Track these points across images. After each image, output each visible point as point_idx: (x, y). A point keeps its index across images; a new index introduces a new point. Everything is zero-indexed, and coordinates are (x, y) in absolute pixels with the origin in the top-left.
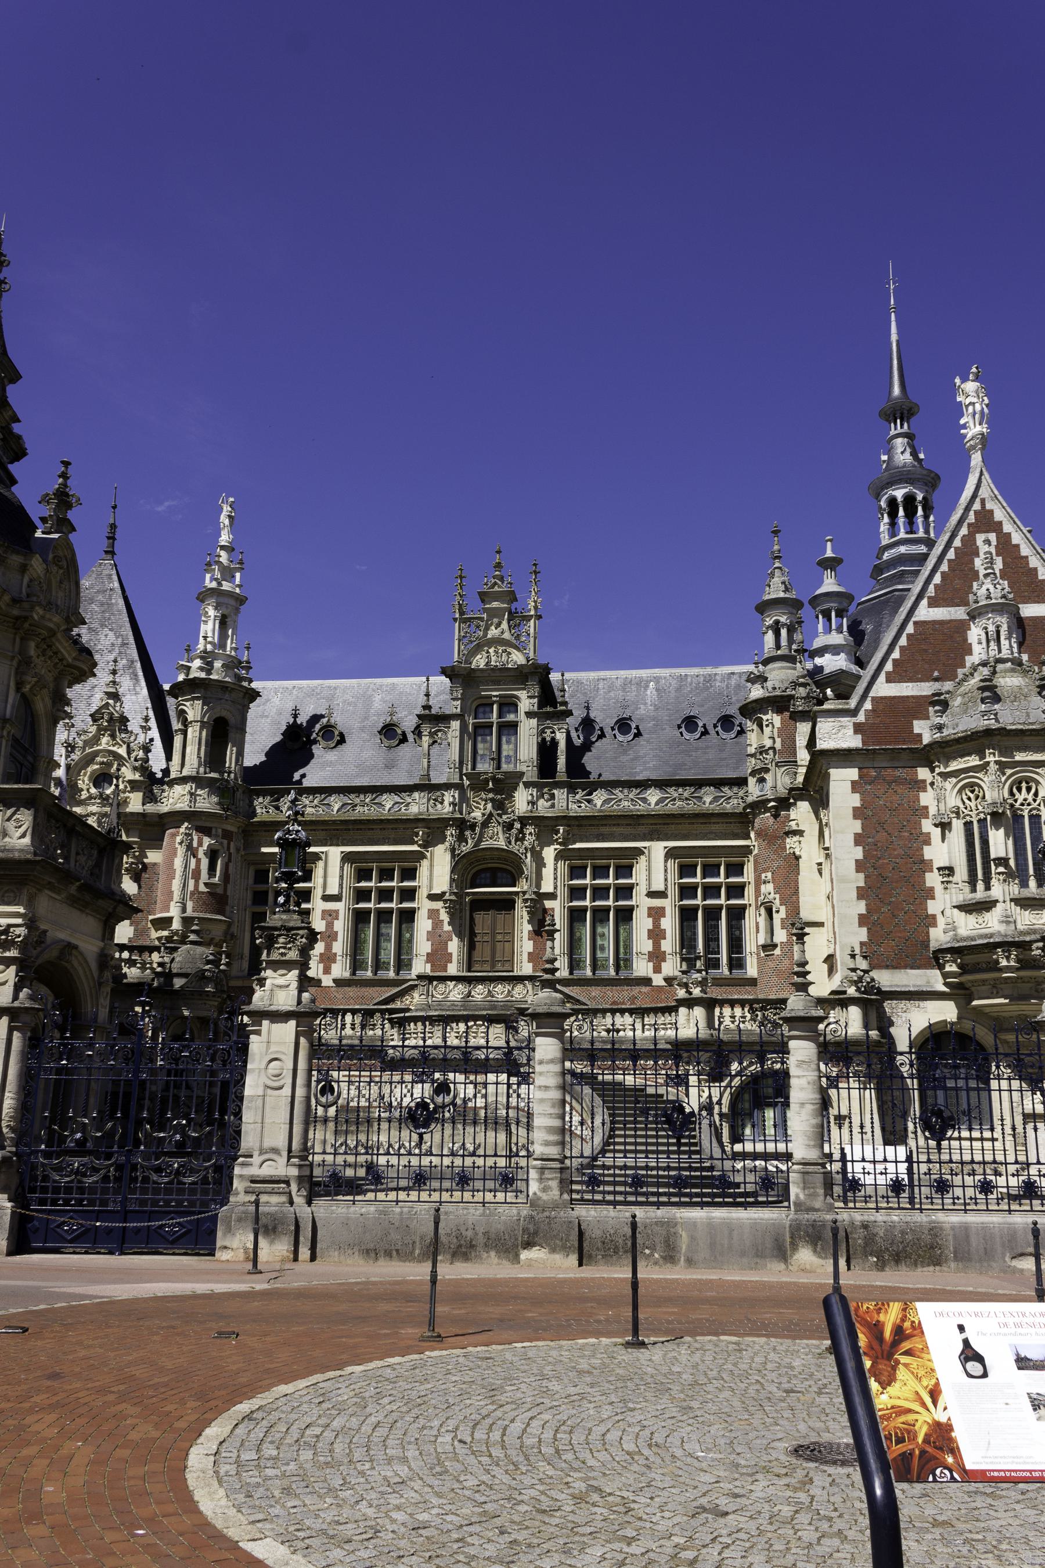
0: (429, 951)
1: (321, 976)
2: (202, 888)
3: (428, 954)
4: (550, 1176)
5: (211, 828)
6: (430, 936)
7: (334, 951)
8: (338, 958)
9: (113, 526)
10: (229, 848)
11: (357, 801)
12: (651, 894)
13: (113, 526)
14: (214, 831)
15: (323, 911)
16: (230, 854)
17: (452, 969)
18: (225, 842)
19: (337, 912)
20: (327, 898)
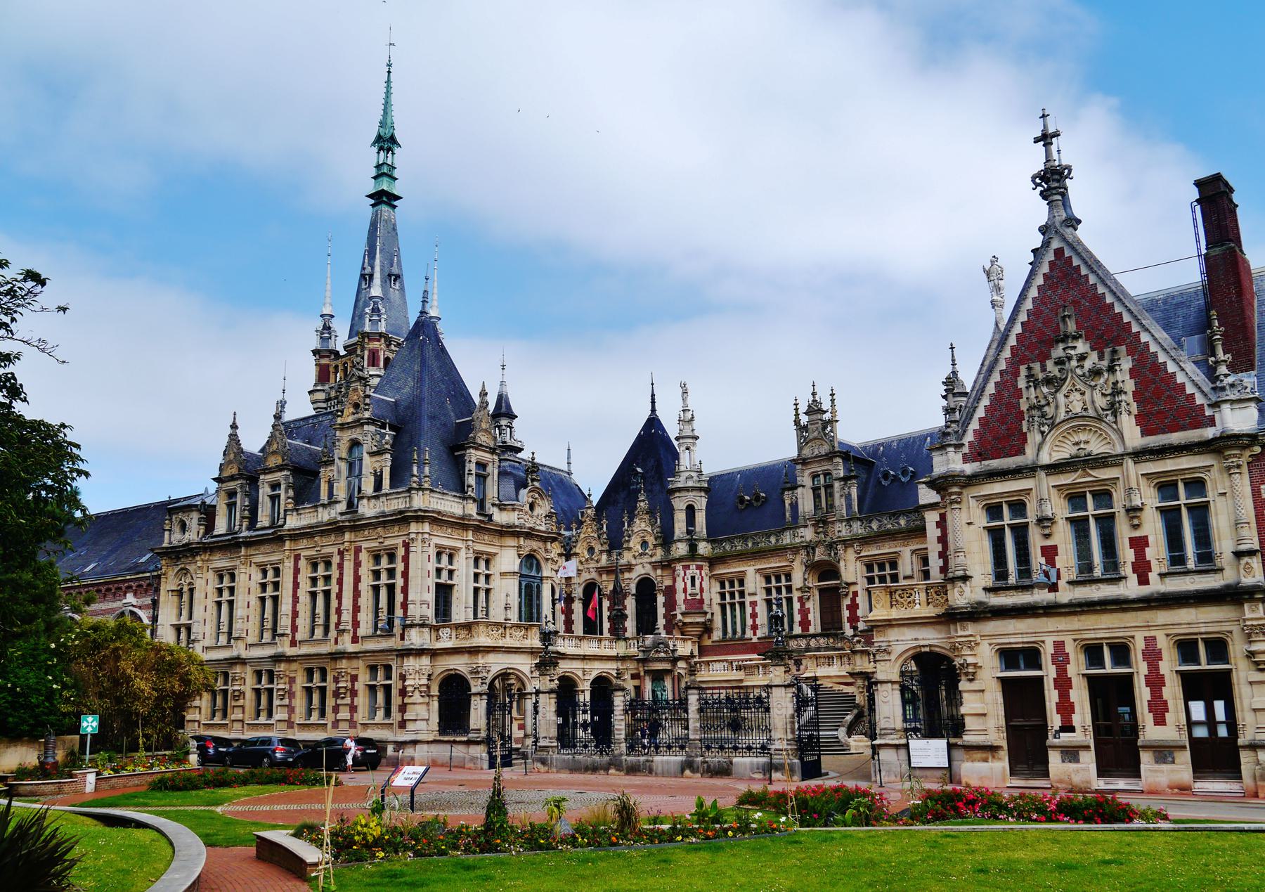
6: (800, 611)
9: (653, 395)
12: (905, 578)
13: (653, 395)
17: (812, 630)
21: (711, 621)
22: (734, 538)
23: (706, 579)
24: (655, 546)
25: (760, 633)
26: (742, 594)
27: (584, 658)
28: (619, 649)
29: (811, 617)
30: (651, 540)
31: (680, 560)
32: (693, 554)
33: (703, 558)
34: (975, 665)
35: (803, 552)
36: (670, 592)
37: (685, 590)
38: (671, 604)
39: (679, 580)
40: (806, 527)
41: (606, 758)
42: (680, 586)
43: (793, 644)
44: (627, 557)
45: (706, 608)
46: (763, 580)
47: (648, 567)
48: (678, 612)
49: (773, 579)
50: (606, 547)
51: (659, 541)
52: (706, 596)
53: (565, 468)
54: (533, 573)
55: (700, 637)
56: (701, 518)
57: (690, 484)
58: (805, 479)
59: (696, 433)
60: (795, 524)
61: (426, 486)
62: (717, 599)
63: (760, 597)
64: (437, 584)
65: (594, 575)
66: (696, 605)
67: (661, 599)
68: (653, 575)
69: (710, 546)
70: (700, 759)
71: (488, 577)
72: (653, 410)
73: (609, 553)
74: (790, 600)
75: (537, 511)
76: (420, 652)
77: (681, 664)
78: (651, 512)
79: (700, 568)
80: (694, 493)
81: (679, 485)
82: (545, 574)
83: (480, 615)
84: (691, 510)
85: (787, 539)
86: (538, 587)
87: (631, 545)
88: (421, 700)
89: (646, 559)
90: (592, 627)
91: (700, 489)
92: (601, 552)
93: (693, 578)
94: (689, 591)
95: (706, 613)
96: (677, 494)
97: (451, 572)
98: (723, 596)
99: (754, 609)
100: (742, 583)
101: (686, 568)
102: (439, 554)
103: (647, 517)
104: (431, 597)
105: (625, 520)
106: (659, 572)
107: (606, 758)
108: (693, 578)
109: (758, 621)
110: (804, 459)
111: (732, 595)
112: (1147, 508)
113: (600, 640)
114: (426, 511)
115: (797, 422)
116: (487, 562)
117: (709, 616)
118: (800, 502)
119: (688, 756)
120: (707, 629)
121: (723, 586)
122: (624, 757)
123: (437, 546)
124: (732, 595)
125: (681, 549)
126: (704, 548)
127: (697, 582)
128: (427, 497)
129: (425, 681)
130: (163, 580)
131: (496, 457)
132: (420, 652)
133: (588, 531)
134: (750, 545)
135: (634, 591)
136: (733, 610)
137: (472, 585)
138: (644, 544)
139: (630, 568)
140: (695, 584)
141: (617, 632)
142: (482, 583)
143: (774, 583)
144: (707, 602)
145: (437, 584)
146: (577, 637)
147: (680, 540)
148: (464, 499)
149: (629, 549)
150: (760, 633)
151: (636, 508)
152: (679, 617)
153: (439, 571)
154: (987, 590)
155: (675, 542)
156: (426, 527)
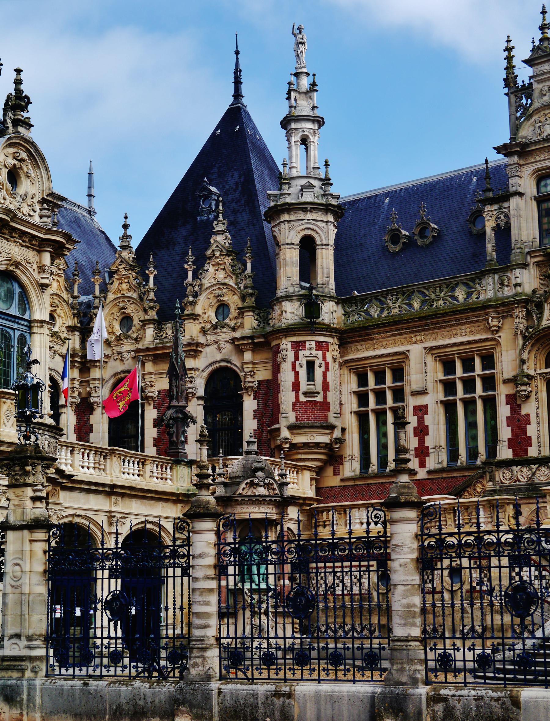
0: (510, 436)
1: (417, 468)
2: (302, 399)
3: (509, 439)
4: (198, 654)
5: (305, 342)
6: (510, 421)
7: (427, 444)
8: (431, 451)
9: (237, 72)
10: (324, 358)
11: (433, 296)
13: (237, 72)
14: (308, 343)
15: (415, 407)
16: (327, 364)
18: (320, 353)
19: (426, 406)
20: (415, 394)
21: (340, 441)
22: (385, 294)
23: (334, 367)
24: (241, 312)
25: (431, 463)
26: (399, 394)
27: (112, 491)
28: (181, 480)
29: (531, 430)
30: (233, 301)
31: (289, 331)
32: (311, 323)
33: (328, 330)
35: (520, 313)
36: (268, 392)
37: (296, 386)
38: (269, 412)
39: (286, 367)
40: (525, 266)
41: (167, 689)
42: (286, 377)
43: (503, 476)
44: (191, 330)
45: (331, 418)
46: (440, 367)
47: (227, 348)
48: (283, 424)
49: (459, 366)
50: (152, 314)
51: (250, 301)
52: (331, 396)
53: (84, 203)
54: (14, 310)
55: (319, 471)
56: (326, 260)
57: (308, 197)
58: (525, 182)
59: (318, 113)
60: (506, 261)
62: (352, 404)
63: (434, 398)
65: (129, 364)
66: (315, 414)
67: (250, 404)
68: (236, 361)
69: (340, 311)
70: (423, 690)
72: (238, 95)
73: (159, 324)
74: (490, 403)
75: (24, 187)
77: (293, 512)
78: (236, 252)
79: (323, 347)
80: (315, 215)
81: (289, 200)
82: (37, 315)
84: (308, 246)
85: (489, 290)
86: (22, 341)
87: (198, 309)
89: (224, 335)
90: (125, 434)
91: (326, 208)
92: (144, 323)
93: (311, 365)
94: (304, 387)
95: (332, 427)
96: (285, 217)
98: (362, 399)
99: (421, 420)
100: (399, 374)
101: (298, 346)
103: (228, 261)
105: (190, 269)
106: (248, 356)
107: (167, 689)
108: (311, 365)
109: (429, 441)
110: (524, 146)
111: (380, 396)
113: (142, 462)
115: (510, 81)
117: (337, 433)
118: (514, 222)
119: (387, 682)
120: (333, 456)
121: (362, 381)
122: (215, 685)
124: (380, 396)
125: (291, 312)
126: (331, 313)
127: (319, 372)
133: (122, 287)
134: (417, 305)
135: (201, 392)
136: (381, 422)
138: (222, 308)
139: (194, 349)
140: (317, 374)
141: (171, 451)
143: (459, 372)
144: (334, 407)
146: (99, 451)
147: (288, 297)
149: (194, 317)
150: (431, 463)
151: (208, 245)
152: (285, 433)
155: (279, 300)
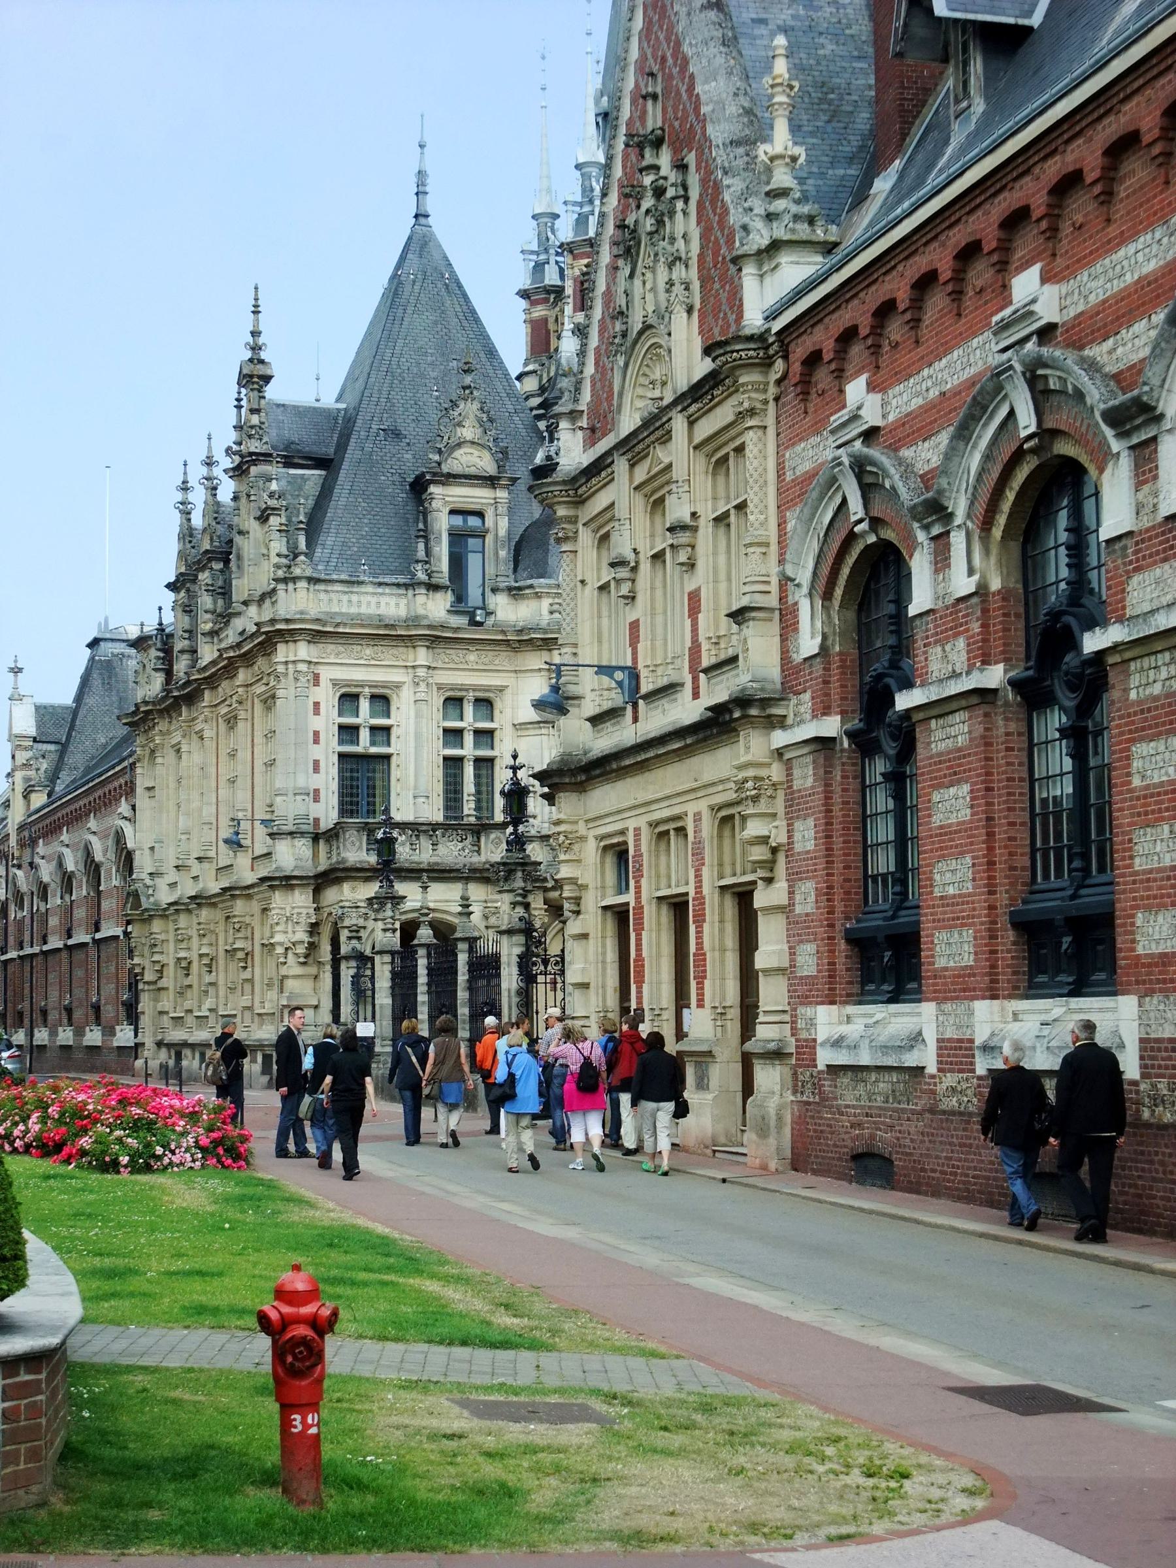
34: (573, 881)
61: (297, 571)
64: (342, 756)
71: (485, 736)
76: (286, 882)
83: (469, 807)
88: (299, 970)
97: (382, 733)
102: (349, 699)
104: (329, 781)
112: (702, 522)
114: (287, 621)
116: (485, 704)
123: (335, 683)
128: (302, 594)
129: (305, 937)
130: (139, 771)
131: (502, 494)
132: (286, 882)
137: (436, 750)
142: (468, 749)
145: (342, 756)
148: (406, 586)
153: (348, 732)
154: (596, 720)
156: (303, 650)
